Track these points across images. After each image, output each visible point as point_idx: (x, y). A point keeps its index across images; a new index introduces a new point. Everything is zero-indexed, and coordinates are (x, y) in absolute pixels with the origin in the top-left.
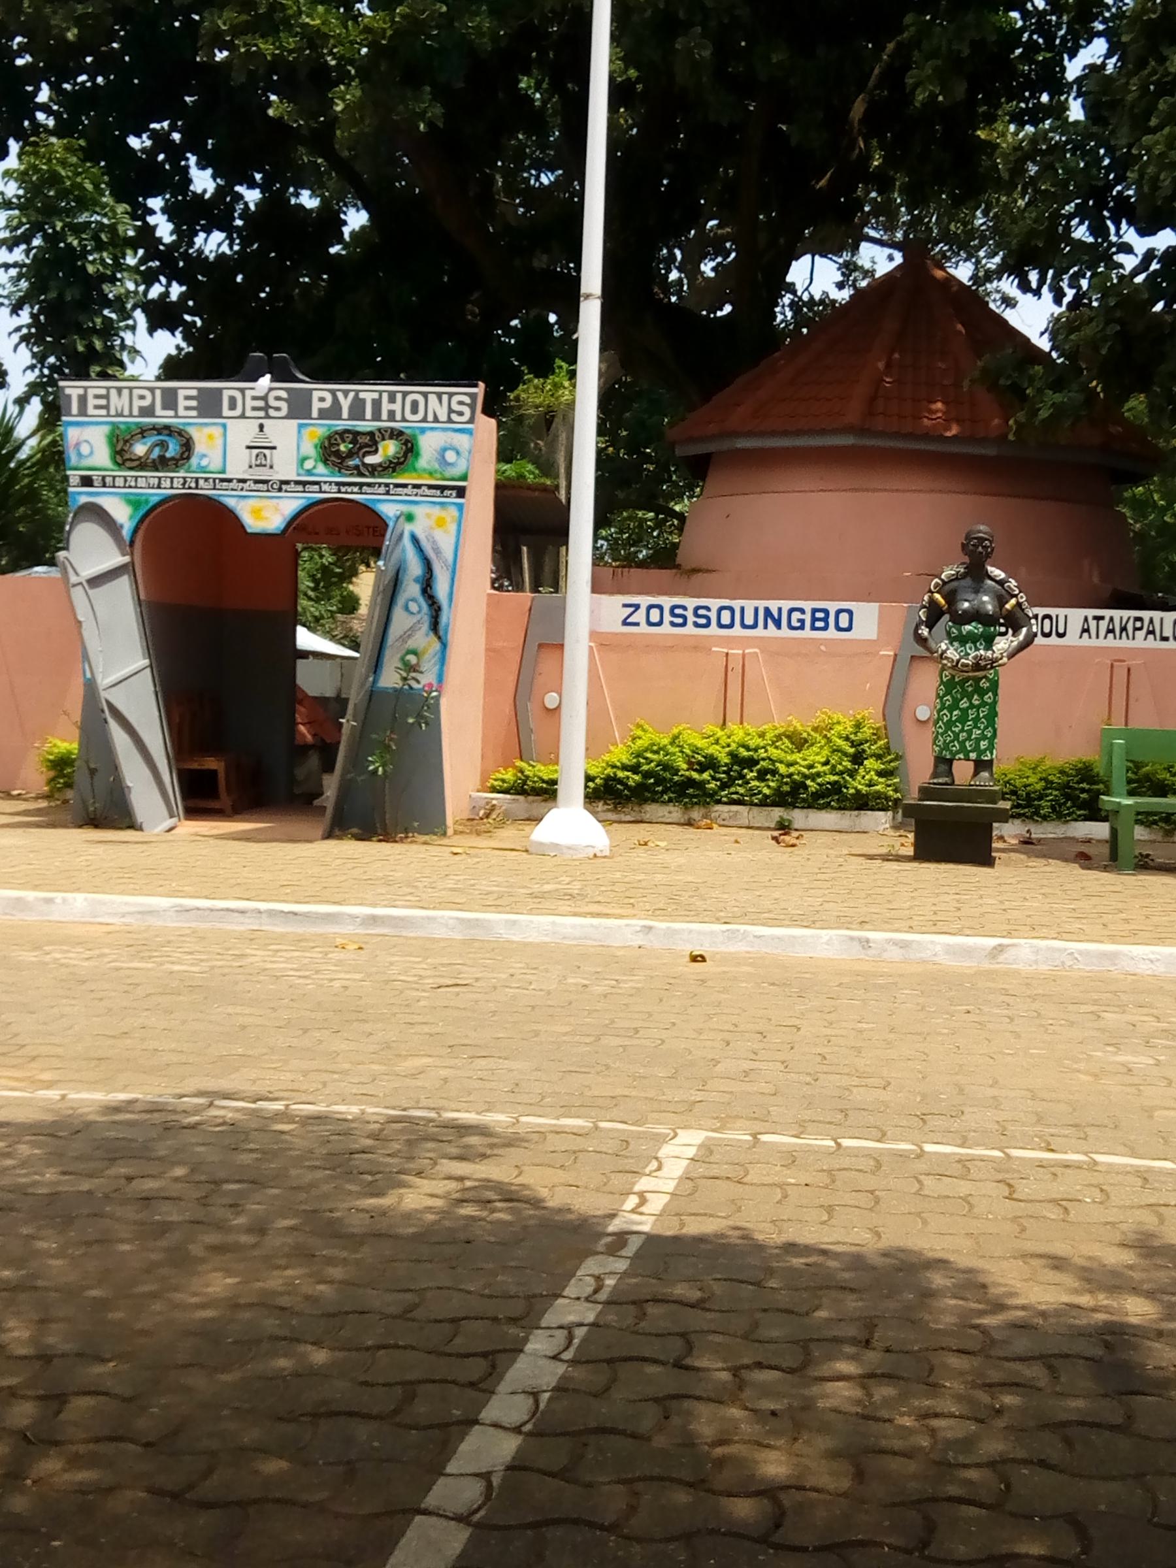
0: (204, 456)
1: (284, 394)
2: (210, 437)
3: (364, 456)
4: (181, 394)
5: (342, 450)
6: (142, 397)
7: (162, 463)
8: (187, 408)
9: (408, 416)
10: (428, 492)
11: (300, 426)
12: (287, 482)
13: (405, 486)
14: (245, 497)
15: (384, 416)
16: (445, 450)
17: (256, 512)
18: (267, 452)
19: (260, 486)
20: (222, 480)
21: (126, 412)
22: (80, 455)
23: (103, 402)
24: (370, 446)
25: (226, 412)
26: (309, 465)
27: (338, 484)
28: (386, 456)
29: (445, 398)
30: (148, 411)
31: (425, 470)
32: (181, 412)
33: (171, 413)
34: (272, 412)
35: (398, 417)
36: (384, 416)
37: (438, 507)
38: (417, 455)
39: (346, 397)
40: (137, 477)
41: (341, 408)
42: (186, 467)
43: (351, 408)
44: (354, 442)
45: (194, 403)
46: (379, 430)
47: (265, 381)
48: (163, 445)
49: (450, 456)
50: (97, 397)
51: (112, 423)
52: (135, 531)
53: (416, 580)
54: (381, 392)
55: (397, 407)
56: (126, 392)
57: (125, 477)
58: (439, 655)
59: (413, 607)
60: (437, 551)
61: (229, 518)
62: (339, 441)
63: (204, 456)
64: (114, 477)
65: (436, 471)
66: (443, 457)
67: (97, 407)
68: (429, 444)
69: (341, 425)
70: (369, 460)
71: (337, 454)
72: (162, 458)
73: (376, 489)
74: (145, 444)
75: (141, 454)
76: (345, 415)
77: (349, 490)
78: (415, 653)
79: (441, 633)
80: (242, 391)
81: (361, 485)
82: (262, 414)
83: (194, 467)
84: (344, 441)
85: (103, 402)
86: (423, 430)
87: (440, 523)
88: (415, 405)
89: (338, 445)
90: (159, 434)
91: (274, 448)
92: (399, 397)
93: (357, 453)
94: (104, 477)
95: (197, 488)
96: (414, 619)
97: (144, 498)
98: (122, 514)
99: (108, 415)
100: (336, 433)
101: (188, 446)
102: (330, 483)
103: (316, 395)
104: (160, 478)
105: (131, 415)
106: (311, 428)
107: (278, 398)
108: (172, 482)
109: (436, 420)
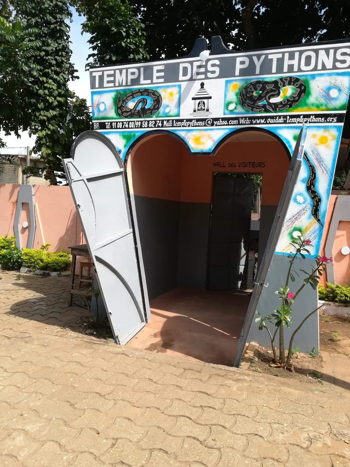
0: (168, 106)
1: (217, 62)
2: (171, 94)
3: (269, 99)
4: (155, 68)
5: (252, 96)
6: (133, 73)
7: (143, 113)
8: (158, 78)
9: (303, 67)
10: (315, 120)
11: (227, 82)
12: (217, 119)
13: (298, 116)
14: (191, 130)
15: (285, 69)
16: (329, 88)
17: (197, 140)
18: (205, 101)
19: (200, 123)
20: (177, 121)
21: (124, 84)
22: (99, 111)
23: (112, 79)
24: (275, 91)
25: (181, 78)
26: (232, 107)
27: (250, 118)
28: (286, 97)
29: (332, 51)
30: (135, 81)
31: (313, 105)
32: (155, 80)
33: (149, 81)
34: (209, 75)
35: (296, 69)
36: (285, 69)
37: (322, 130)
38: (309, 94)
39: (259, 59)
40: (129, 122)
41: (255, 66)
42: (157, 114)
43: (261, 66)
44: (263, 89)
45: (162, 74)
46: (281, 79)
47: (206, 54)
48: (144, 101)
49: (334, 93)
50: (109, 76)
51: (117, 91)
52: (127, 154)
53: (303, 181)
54: (283, 53)
55: (295, 62)
56: (124, 71)
57: (122, 122)
58: (317, 232)
59: (300, 199)
60: (320, 161)
61: (181, 144)
62: (253, 89)
63: (168, 106)
64: (117, 122)
65: (322, 105)
66: (328, 94)
67: (108, 82)
68: (317, 86)
69: (253, 78)
70: (273, 100)
71: (251, 98)
72: (143, 109)
73: (277, 120)
74: (134, 102)
75: (132, 108)
76: (258, 71)
77: (258, 122)
78: (300, 230)
79: (320, 217)
80: (191, 63)
81: (266, 118)
82: (203, 76)
83: (161, 114)
84: (256, 89)
85: (112, 79)
86: (313, 77)
87: (323, 140)
88: (308, 58)
89: (252, 92)
90: (142, 95)
91: (210, 98)
92: (297, 54)
93: (265, 97)
94: (111, 123)
95: (162, 126)
96: (301, 207)
97: (132, 134)
98: (119, 142)
99: (115, 86)
100: (251, 84)
101: (158, 101)
102: (246, 118)
103: (239, 60)
104: (141, 122)
105: (127, 85)
106: (234, 83)
107: (213, 65)
108: (148, 124)
109: (324, 68)
